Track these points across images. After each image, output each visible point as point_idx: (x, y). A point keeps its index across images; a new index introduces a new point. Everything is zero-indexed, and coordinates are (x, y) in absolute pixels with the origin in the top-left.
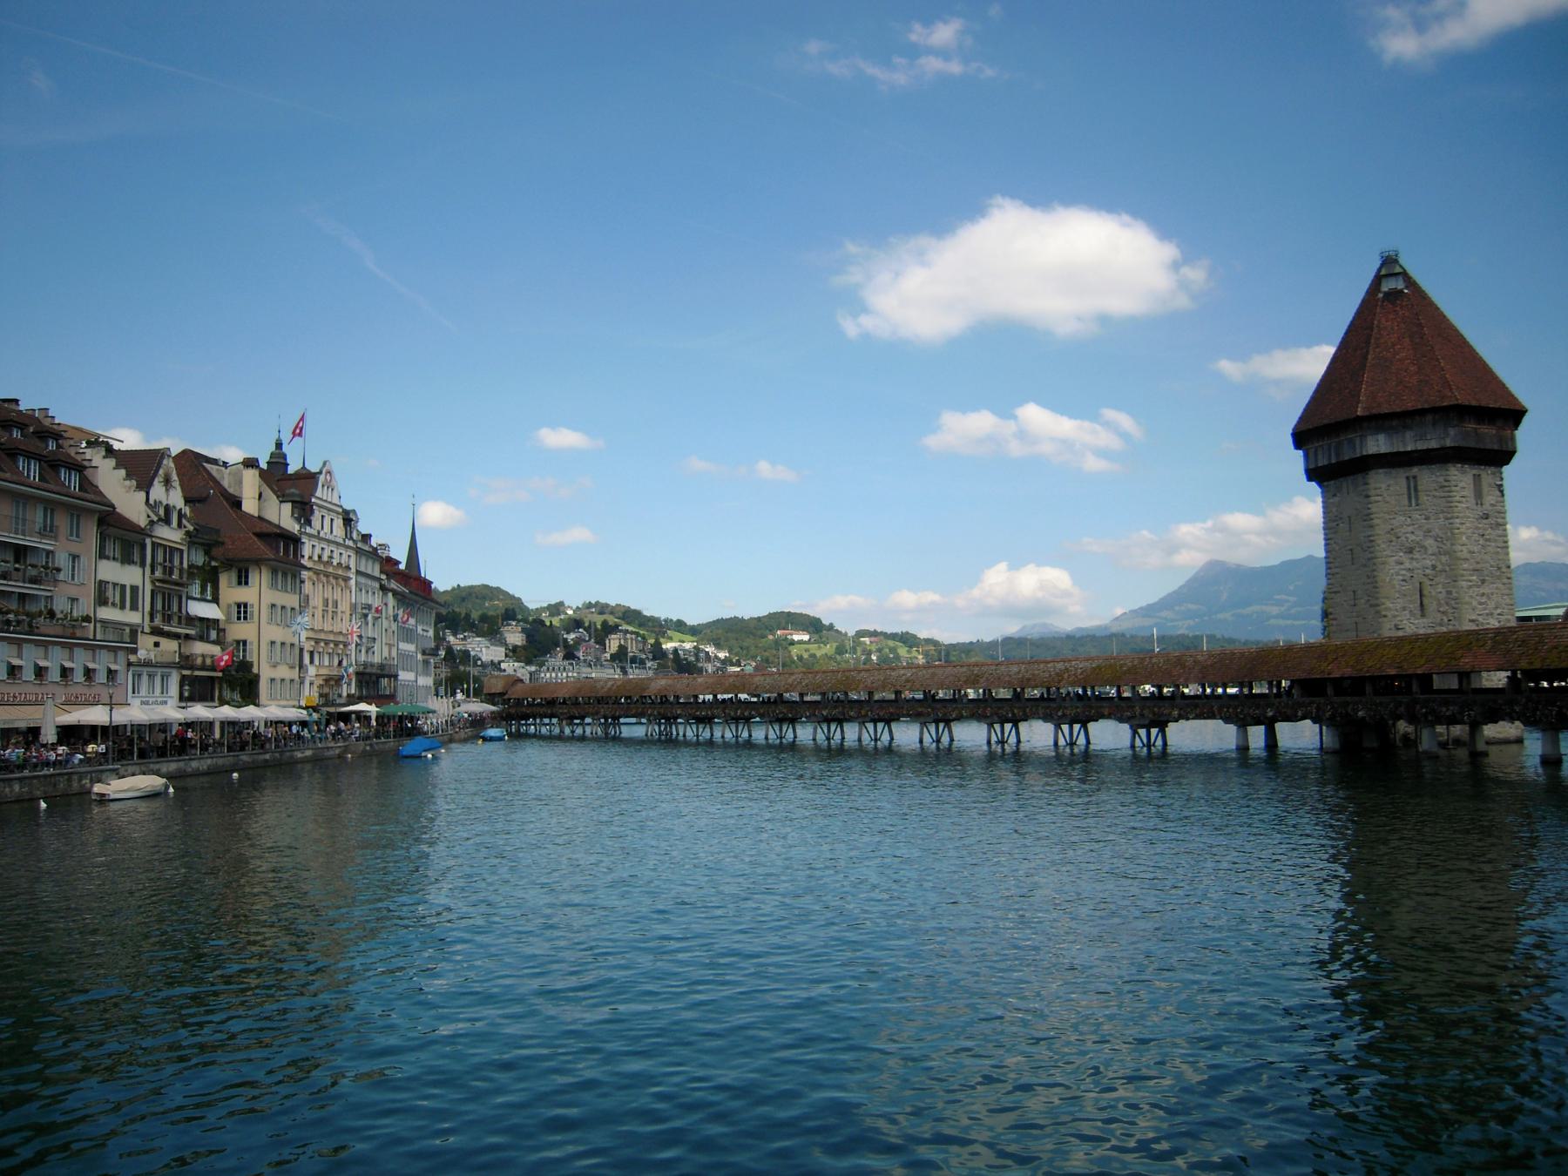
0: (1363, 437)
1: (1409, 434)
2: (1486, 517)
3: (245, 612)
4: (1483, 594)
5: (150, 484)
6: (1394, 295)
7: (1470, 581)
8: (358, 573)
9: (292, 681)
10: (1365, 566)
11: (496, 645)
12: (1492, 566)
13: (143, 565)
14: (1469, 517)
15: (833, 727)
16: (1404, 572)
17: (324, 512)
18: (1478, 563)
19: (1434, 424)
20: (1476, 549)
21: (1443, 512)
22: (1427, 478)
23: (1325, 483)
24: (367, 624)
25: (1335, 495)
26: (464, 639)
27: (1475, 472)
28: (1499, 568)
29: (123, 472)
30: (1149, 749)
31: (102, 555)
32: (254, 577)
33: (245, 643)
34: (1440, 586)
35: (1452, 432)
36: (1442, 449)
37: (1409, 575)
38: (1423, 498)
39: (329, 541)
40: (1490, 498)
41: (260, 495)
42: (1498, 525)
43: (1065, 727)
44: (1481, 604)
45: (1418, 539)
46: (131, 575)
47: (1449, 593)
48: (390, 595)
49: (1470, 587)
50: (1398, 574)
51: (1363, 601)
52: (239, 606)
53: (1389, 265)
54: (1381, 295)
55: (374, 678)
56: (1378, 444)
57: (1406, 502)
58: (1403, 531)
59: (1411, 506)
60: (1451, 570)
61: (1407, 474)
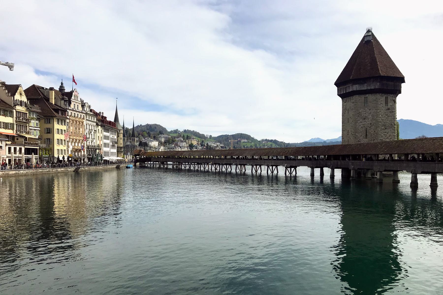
1: (365, 84)
2: (389, 109)
5: (15, 94)
7: (381, 128)
8: (87, 120)
9: (65, 150)
10: (351, 123)
13: (13, 117)
14: (383, 109)
15: (217, 166)
17: (75, 103)
18: (385, 123)
22: (371, 97)
23: (343, 99)
24: (92, 135)
25: (345, 103)
27: (386, 96)
30: (291, 175)
32: (52, 121)
33: (49, 139)
35: (378, 84)
39: (76, 111)
40: (390, 104)
42: (393, 112)
43: (271, 167)
45: (367, 116)
47: (375, 131)
48: (100, 127)
49: (381, 130)
51: (350, 133)
55: (95, 150)
56: (356, 87)
57: (364, 105)
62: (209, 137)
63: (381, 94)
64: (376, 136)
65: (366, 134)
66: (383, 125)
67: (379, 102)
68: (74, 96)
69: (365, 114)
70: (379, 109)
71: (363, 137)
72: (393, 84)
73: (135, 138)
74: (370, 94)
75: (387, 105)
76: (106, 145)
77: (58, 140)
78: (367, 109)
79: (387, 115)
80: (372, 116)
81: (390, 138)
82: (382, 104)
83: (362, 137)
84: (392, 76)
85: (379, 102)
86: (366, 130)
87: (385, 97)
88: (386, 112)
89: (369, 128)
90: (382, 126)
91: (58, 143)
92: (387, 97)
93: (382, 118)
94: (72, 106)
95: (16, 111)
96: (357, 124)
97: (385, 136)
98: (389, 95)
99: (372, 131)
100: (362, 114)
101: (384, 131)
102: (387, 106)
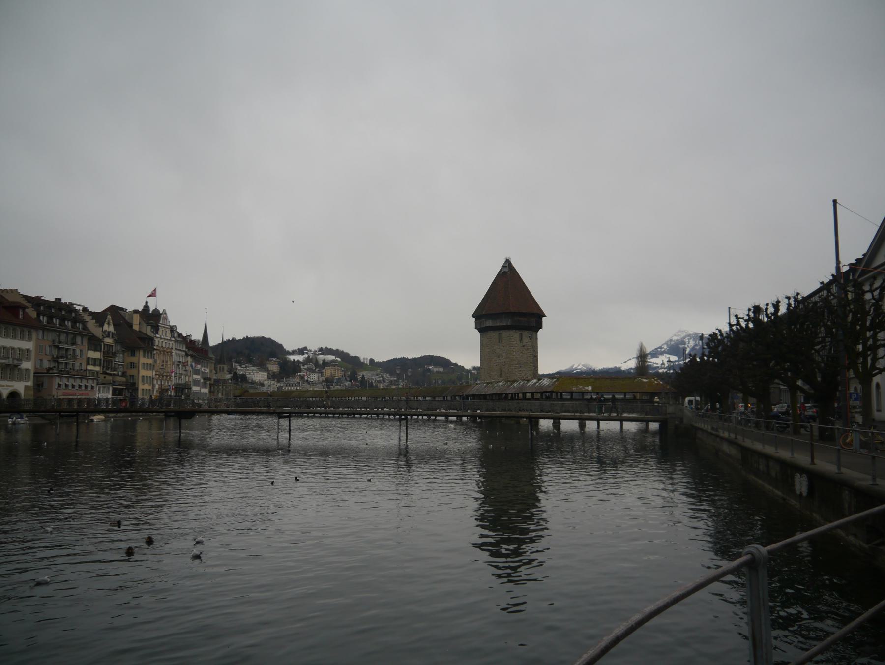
0: (486, 320)
2: (524, 346)
3: (134, 366)
4: (520, 371)
6: (505, 273)
8: (176, 349)
11: (263, 372)
18: (519, 361)
22: (505, 334)
24: (179, 368)
26: (246, 367)
28: (527, 363)
29: (94, 321)
31: (89, 349)
32: (137, 353)
33: (133, 376)
36: (507, 325)
41: (140, 324)
42: (528, 349)
46: (97, 355)
47: (509, 370)
48: (189, 357)
52: (131, 363)
53: (508, 261)
54: (501, 273)
56: (489, 323)
62: (368, 363)
73: (224, 366)
76: (196, 382)
77: (143, 376)
79: (522, 352)
91: (143, 381)
94: (160, 332)
95: (105, 345)
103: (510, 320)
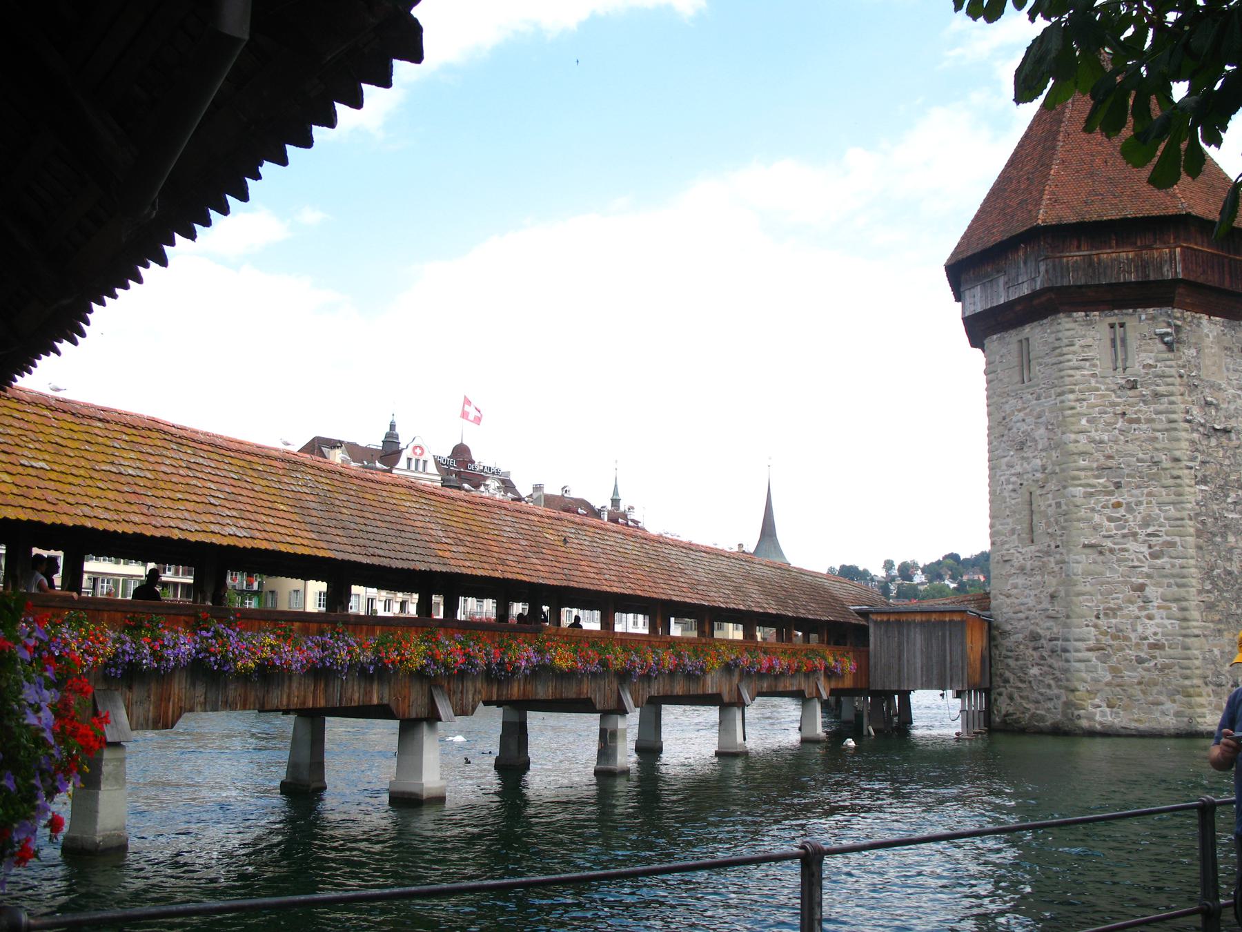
1: (1002, 280)
2: (1133, 386)
4: (1118, 505)
12: (1139, 460)
14: (1098, 389)
16: (1013, 479)
18: (1110, 457)
19: (1025, 263)
20: (1106, 438)
21: (1054, 386)
22: (1037, 334)
34: (1050, 496)
36: (1034, 295)
37: (1019, 482)
38: (1036, 368)
42: (1157, 395)
44: (1110, 519)
45: (1029, 428)
47: (1058, 505)
49: (1091, 495)
50: (1008, 482)
58: (1014, 419)
59: (1024, 383)
60: (1063, 470)
61: (1020, 339)
63: (1083, 314)
64: (1063, 528)
65: (1025, 525)
66: (1102, 468)
67: (1070, 357)
68: (409, 459)
69: (1024, 420)
70: (1072, 392)
71: (1019, 535)
72: (1131, 255)
74: (1036, 323)
75: (1120, 364)
78: (1030, 396)
79: (1124, 414)
80: (1047, 429)
81: (1149, 535)
82: (1095, 366)
83: (1015, 537)
84: (1105, 218)
85: (1074, 353)
86: (1029, 500)
87: (1112, 326)
88: (1119, 400)
89: (1039, 492)
90: (1098, 477)
92: (1122, 325)
93: (1096, 436)
96: (999, 473)
97: (1117, 528)
98: (1131, 315)
99: (1050, 506)
100: (1012, 424)
101: (1107, 501)
102: (1120, 370)
103: (1042, 268)
